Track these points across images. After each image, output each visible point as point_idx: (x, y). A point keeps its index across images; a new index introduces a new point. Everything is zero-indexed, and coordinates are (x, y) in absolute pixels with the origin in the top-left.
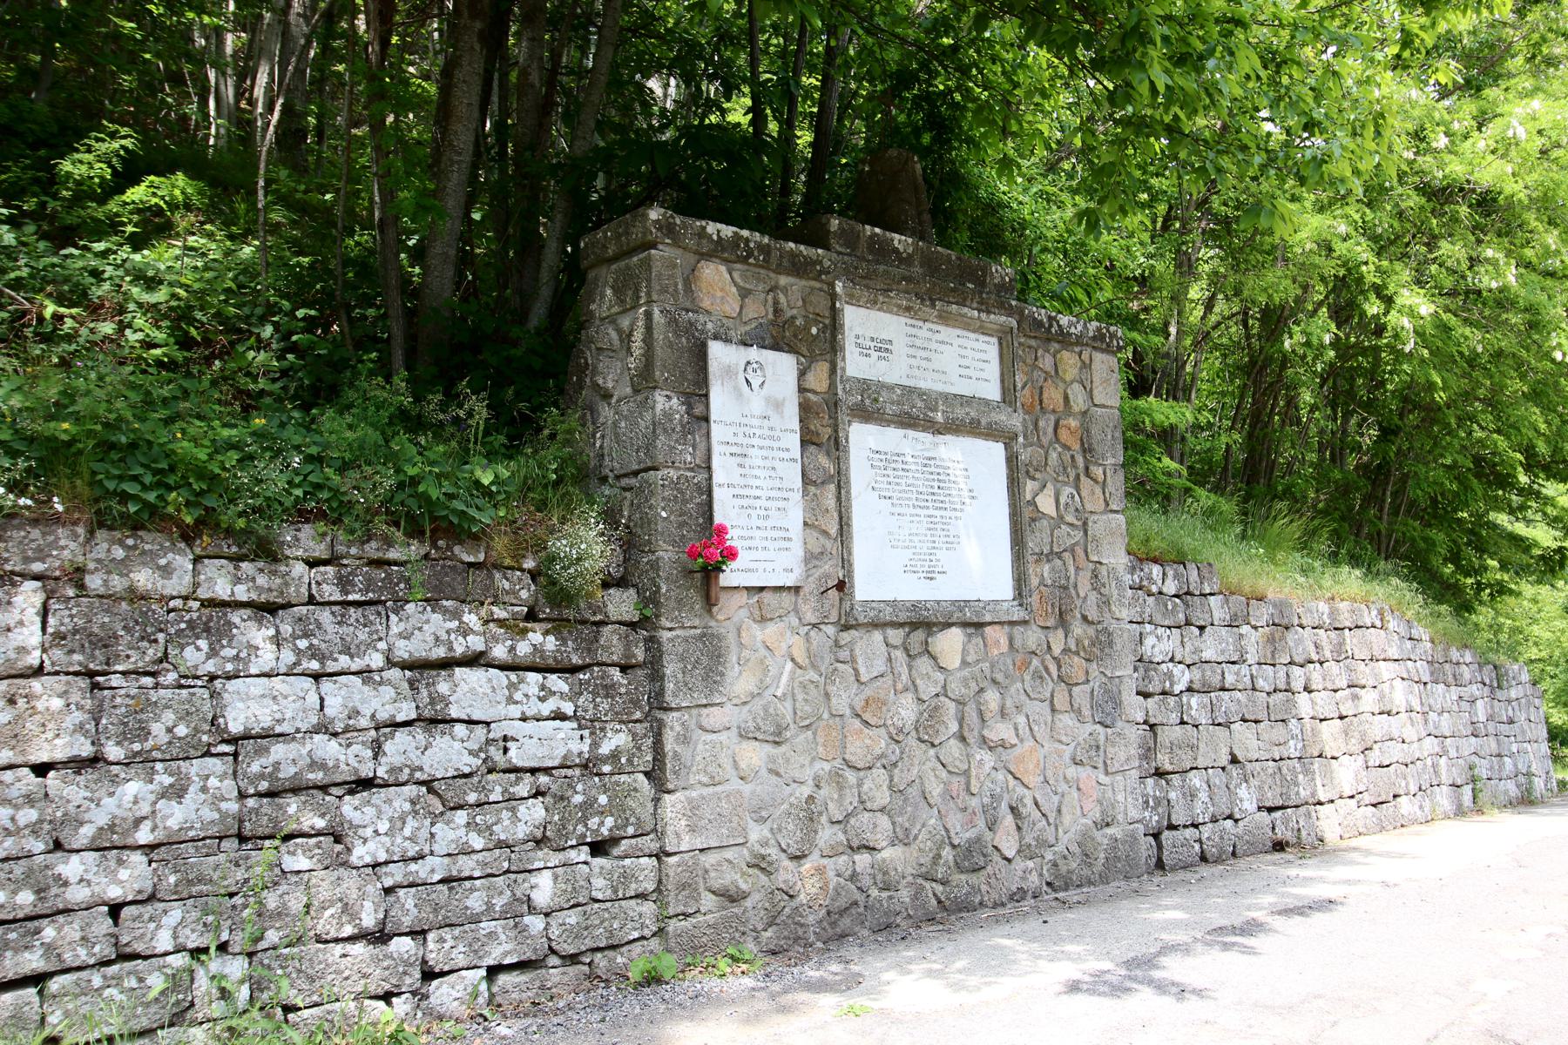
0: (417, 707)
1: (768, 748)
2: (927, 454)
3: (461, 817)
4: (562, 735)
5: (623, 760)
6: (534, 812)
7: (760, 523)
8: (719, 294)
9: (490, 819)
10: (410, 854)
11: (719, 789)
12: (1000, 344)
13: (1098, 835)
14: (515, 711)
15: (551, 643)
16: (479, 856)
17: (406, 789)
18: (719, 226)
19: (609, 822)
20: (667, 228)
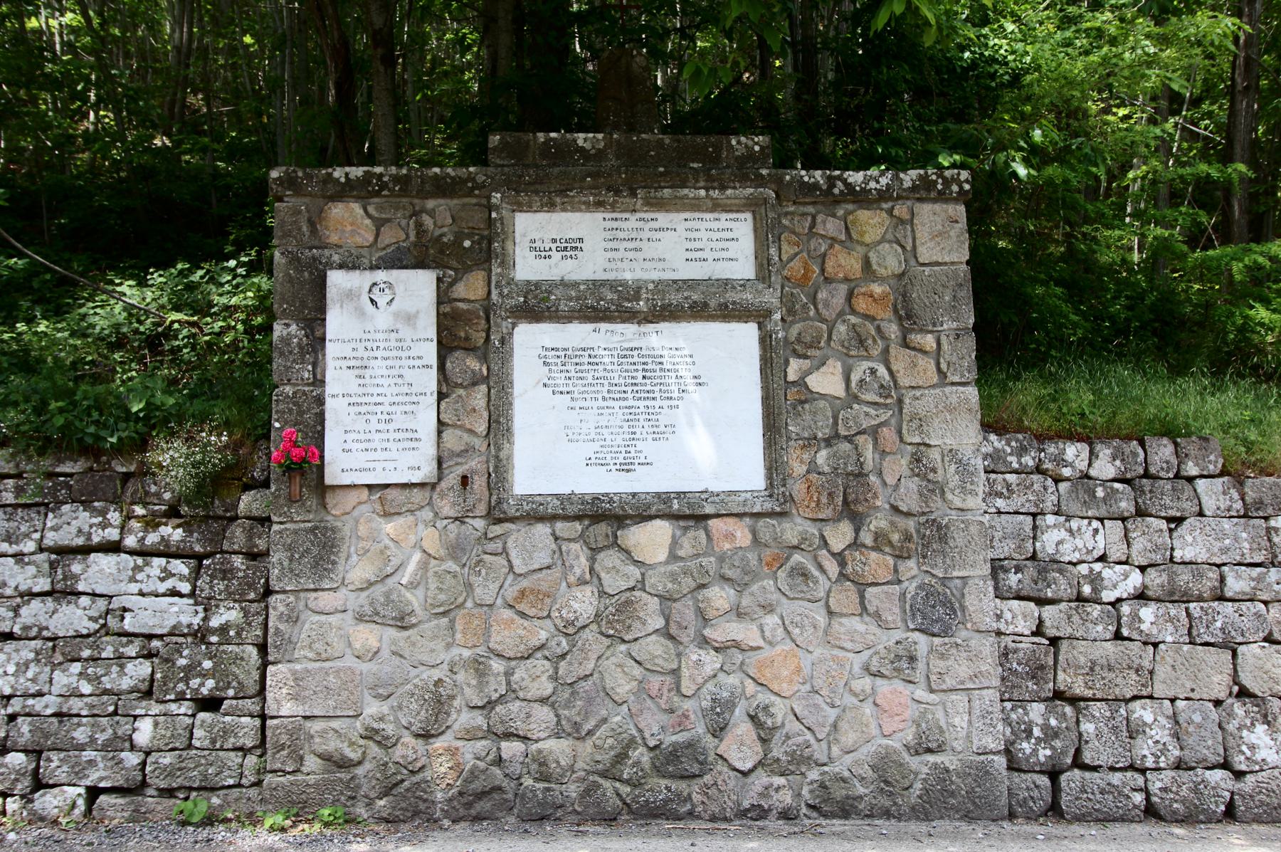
0: (52, 582)
1: (392, 633)
2: (626, 345)
3: (76, 668)
4: (176, 609)
5: (232, 633)
6: (141, 670)
7: (382, 426)
8: (349, 228)
9: (100, 671)
10: (31, 691)
11: (327, 664)
12: (755, 218)
13: (914, 762)
14: (134, 588)
15: (178, 534)
16: (88, 700)
17: (33, 642)
18: (347, 169)
19: (210, 683)
20: (290, 182)
